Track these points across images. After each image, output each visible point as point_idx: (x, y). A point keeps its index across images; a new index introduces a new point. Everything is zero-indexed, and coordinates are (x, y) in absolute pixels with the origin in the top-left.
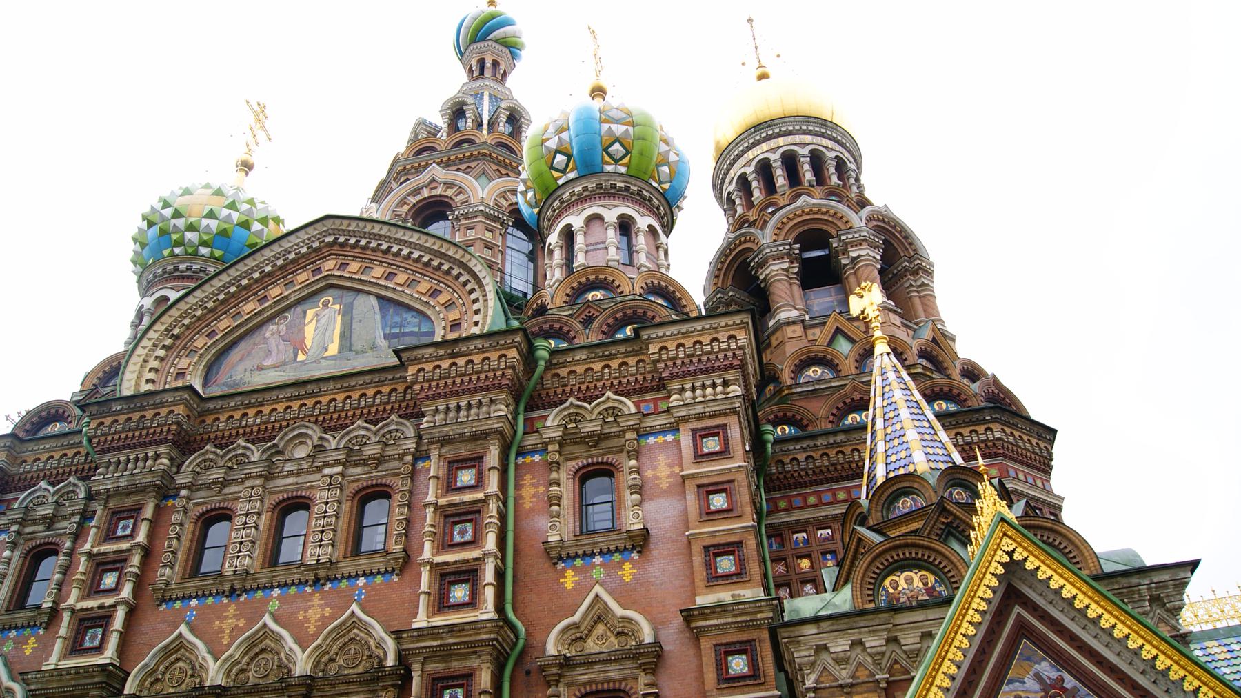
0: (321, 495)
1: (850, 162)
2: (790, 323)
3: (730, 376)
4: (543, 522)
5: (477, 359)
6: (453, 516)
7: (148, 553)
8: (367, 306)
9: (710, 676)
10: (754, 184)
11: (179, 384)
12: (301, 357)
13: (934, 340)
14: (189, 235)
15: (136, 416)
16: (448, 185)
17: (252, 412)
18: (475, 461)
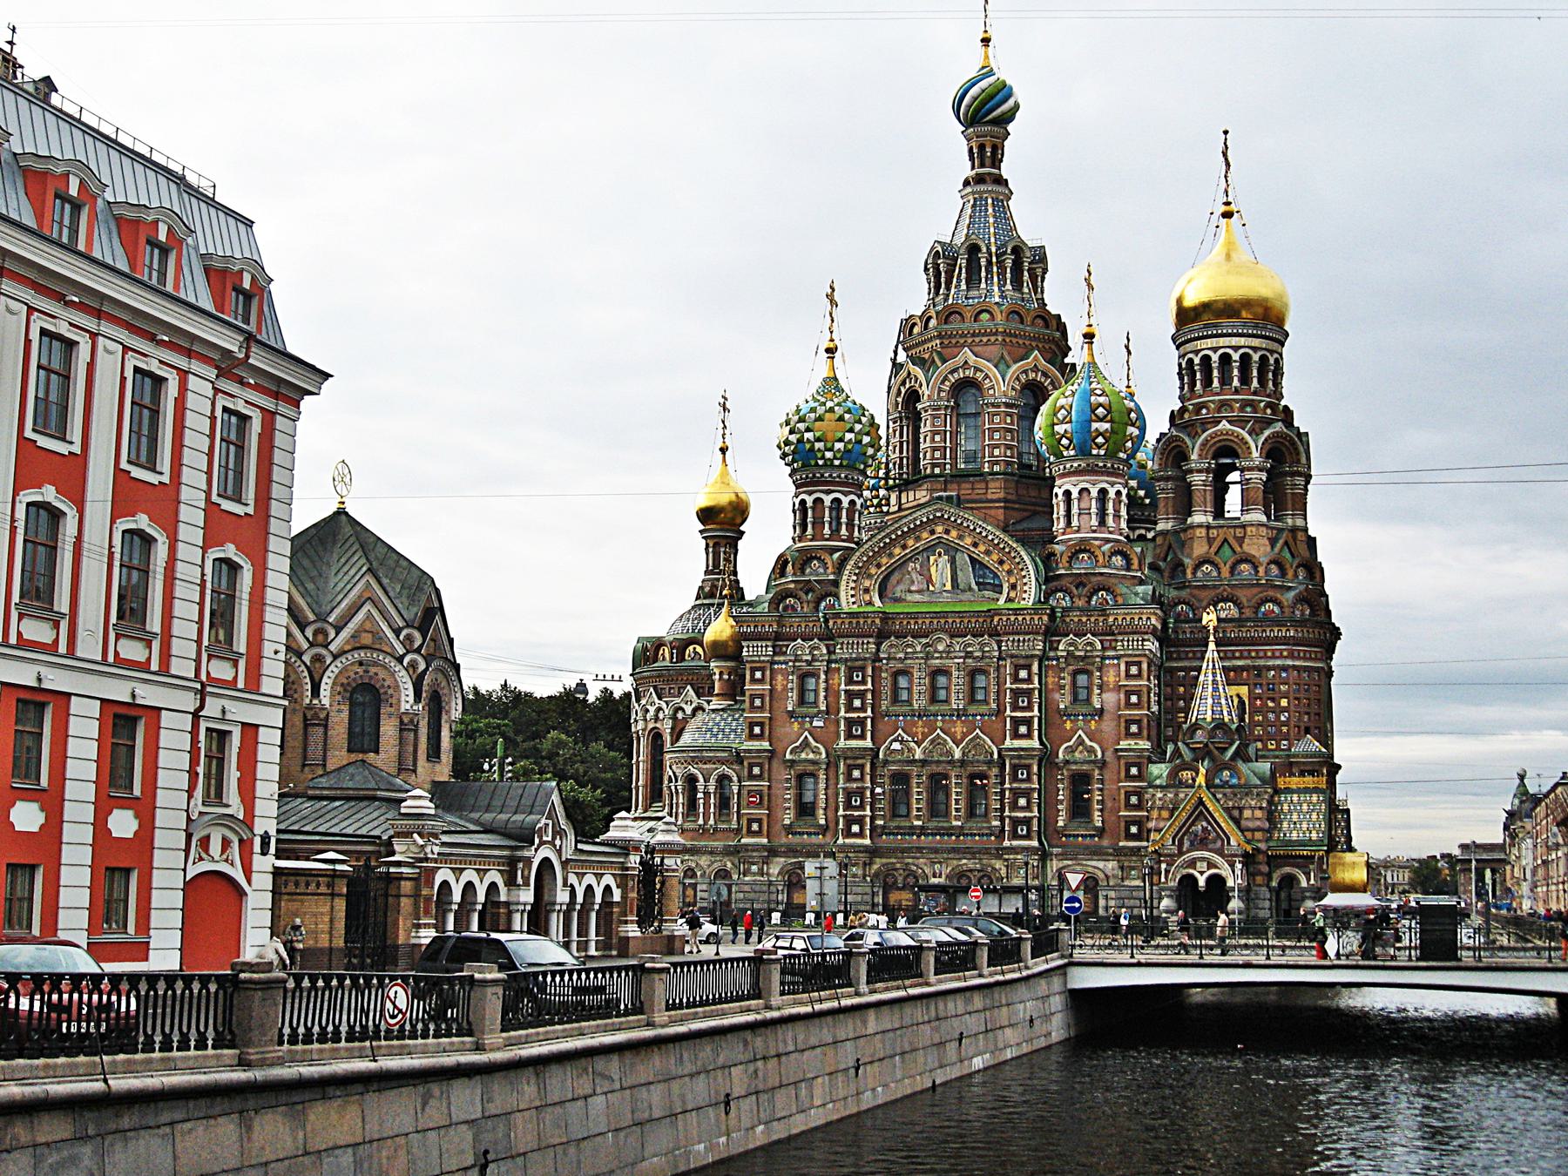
0: (955, 673)
1: (1272, 352)
2: (1200, 526)
3: (1146, 637)
4: (1057, 696)
5: (1028, 618)
6: (1016, 694)
7: (873, 692)
8: (963, 559)
9: (1123, 774)
10: (1198, 376)
11: (867, 597)
12: (931, 588)
13: (1286, 543)
14: (829, 455)
15: (854, 621)
16: (977, 369)
17: (912, 622)
18: (1028, 667)
